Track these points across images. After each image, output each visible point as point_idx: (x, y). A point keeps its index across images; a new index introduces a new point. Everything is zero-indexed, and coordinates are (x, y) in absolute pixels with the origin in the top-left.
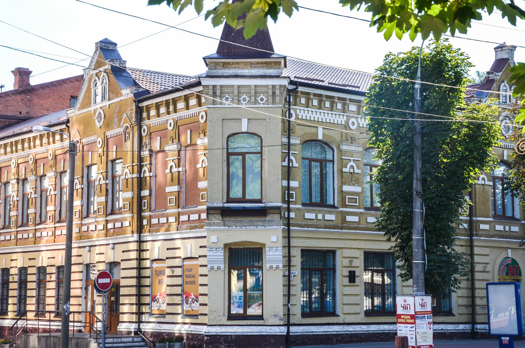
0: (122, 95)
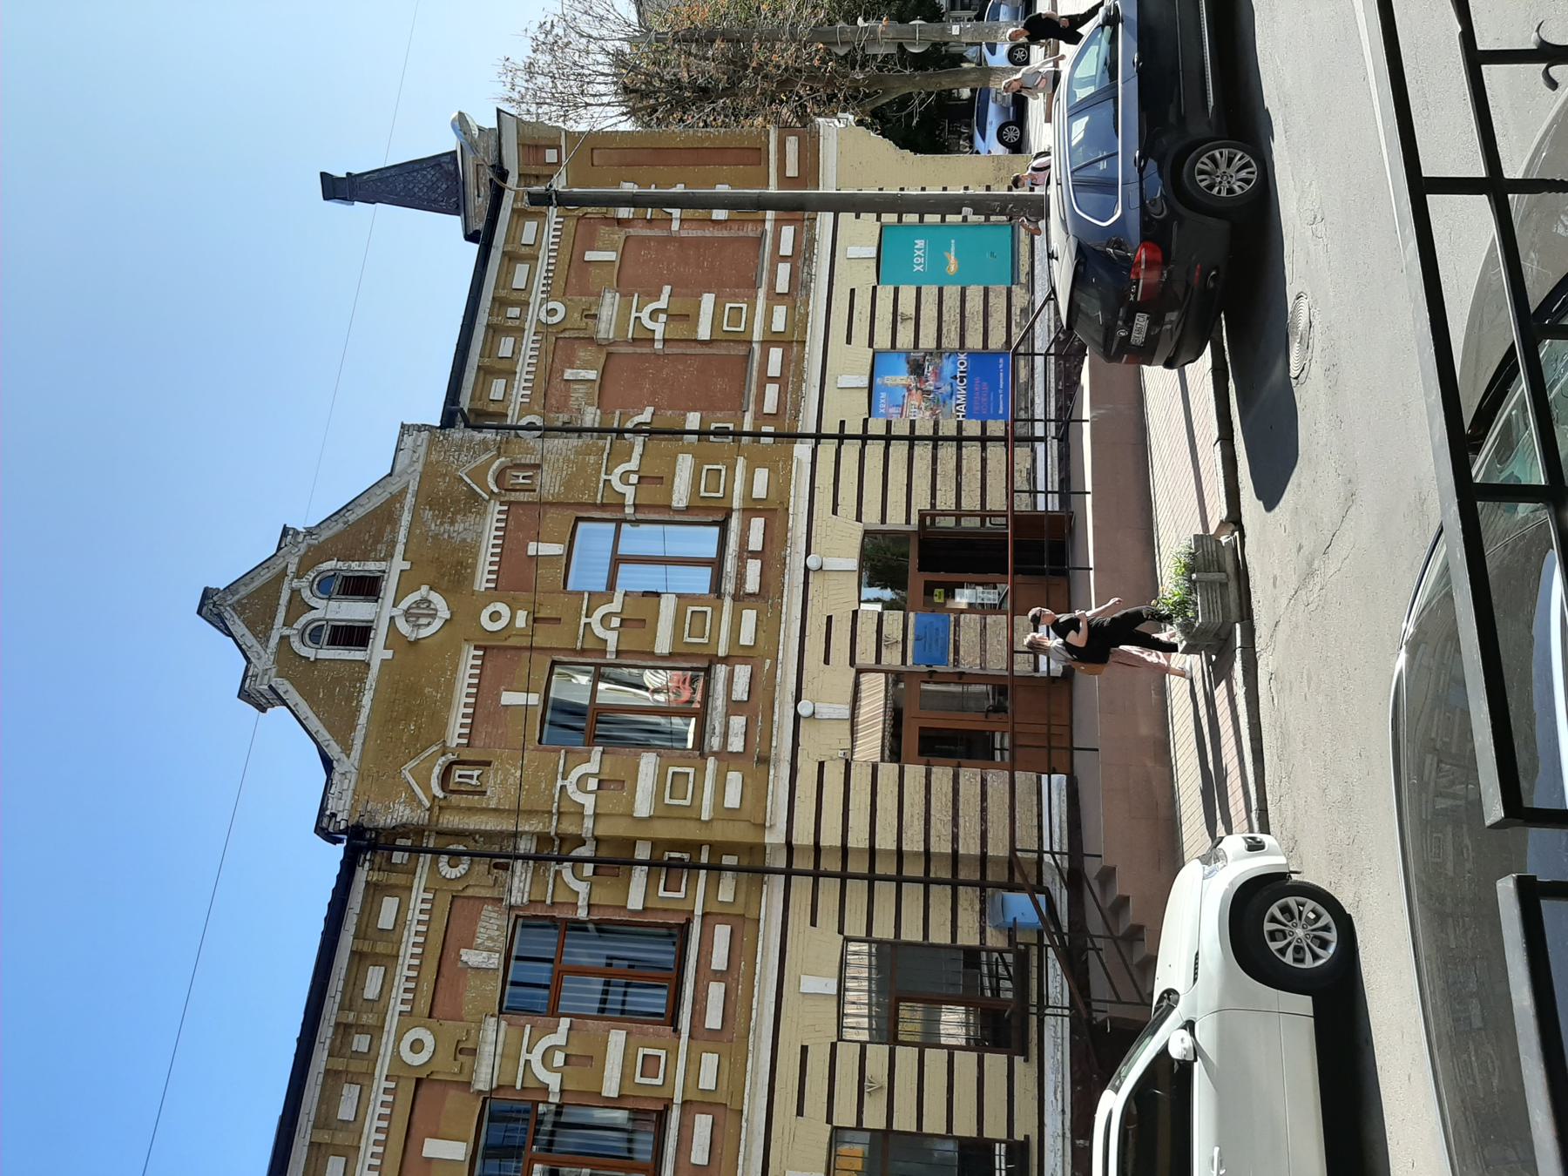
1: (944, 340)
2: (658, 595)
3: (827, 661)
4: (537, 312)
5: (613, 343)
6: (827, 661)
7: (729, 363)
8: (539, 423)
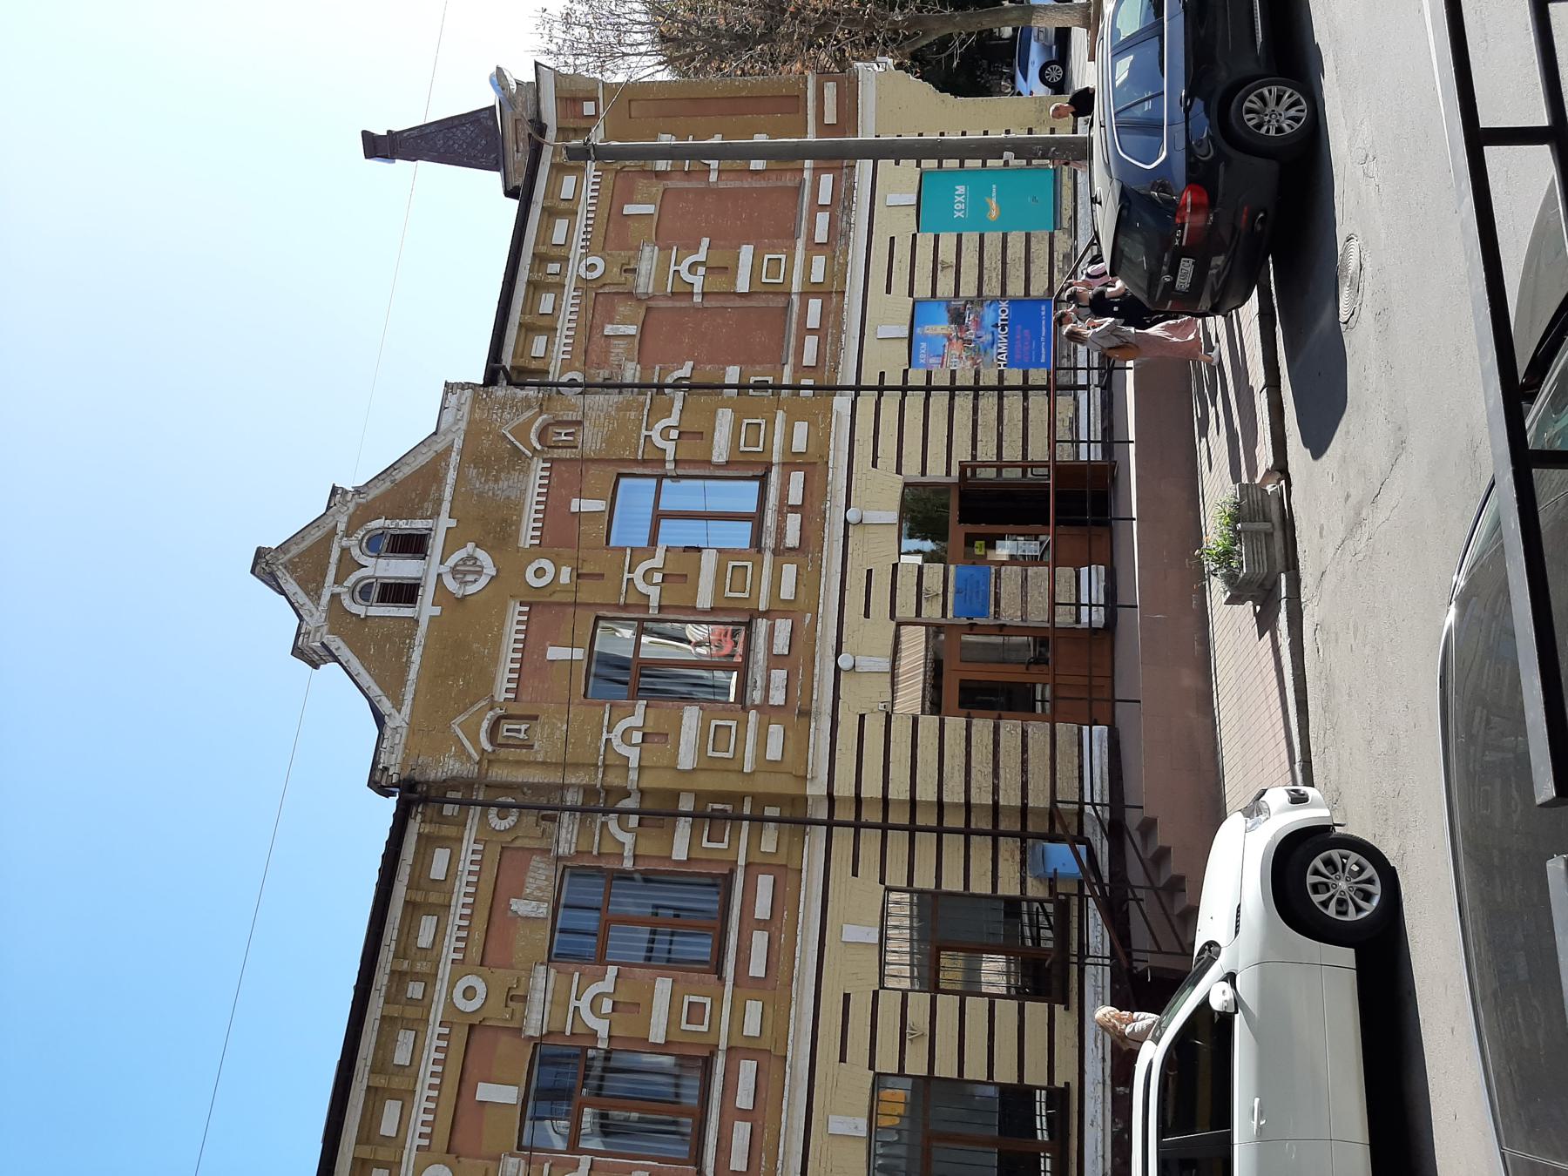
1: (985, 288)
2: (699, 550)
3: (867, 615)
4: (576, 268)
5: (652, 297)
6: (867, 615)
8: (580, 380)
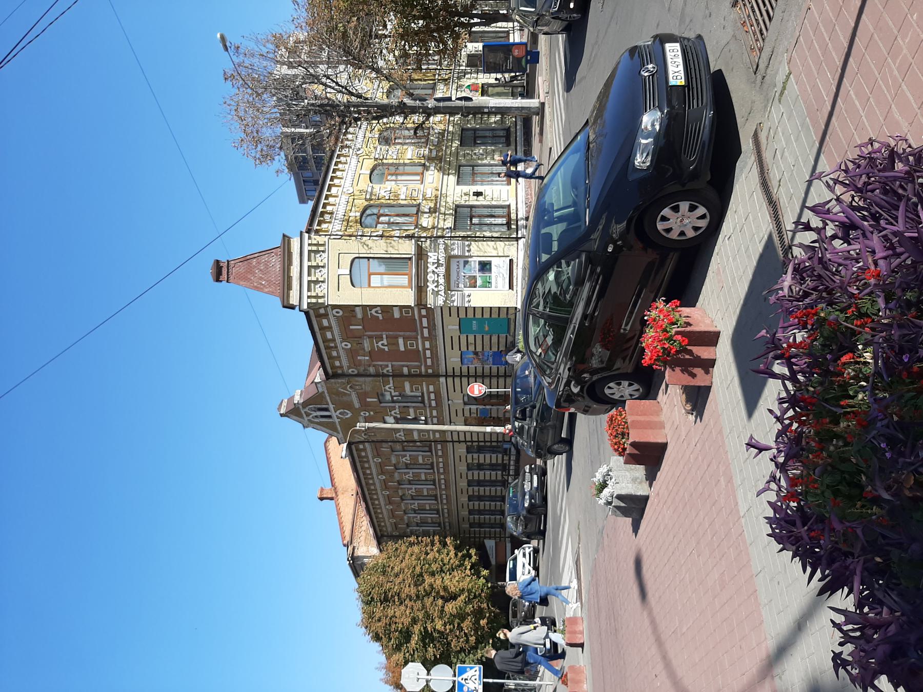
0: (323, 392)
7: (414, 355)
